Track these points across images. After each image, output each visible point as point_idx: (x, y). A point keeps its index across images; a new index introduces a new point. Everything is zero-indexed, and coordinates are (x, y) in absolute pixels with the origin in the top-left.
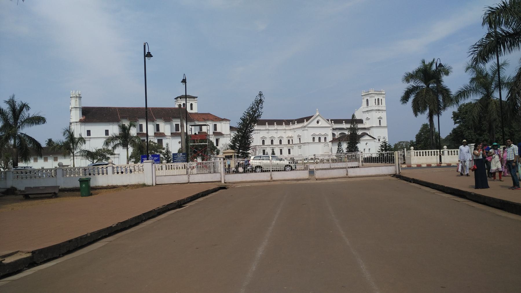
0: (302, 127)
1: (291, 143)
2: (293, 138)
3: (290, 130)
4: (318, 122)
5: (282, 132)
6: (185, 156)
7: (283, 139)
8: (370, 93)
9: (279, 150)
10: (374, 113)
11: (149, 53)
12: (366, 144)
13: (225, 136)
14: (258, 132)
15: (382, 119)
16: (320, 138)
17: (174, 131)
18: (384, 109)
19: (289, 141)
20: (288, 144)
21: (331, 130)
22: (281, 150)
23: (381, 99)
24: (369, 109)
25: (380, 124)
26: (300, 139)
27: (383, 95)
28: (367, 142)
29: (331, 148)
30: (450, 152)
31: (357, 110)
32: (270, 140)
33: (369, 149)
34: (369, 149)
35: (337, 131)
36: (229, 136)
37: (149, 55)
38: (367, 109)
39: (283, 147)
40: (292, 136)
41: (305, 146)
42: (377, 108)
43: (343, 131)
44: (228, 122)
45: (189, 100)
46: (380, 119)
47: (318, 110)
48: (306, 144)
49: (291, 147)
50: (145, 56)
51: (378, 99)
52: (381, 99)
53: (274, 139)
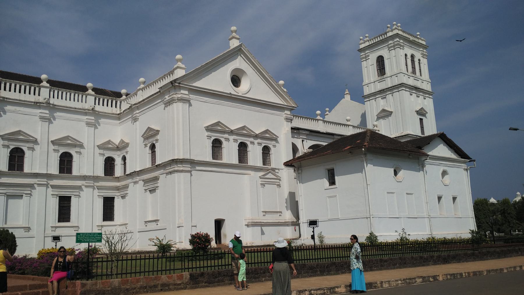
0: (161, 93)
2: (128, 149)
3: (119, 117)
4: (236, 80)
5: (80, 120)
7: (80, 153)
8: (390, 34)
10: (405, 94)
16: (243, 148)
18: (427, 87)
20: (106, 174)
23: (419, 60)
24: (389, 83)
25: (423, 132)
26: (153, 147)
27: (421, 49)
28: (446, 168)
29: (292, 195)
31: (330, 111)
32: (4, 146)
34: (454, 199)
38: (380, 86)
39: (79, 188)
40: (122, 141)
41: (176, 175)
42: (411, 82)
46: (421, 113)
47: (235, 32)
48: (180, 167)
49: (118, 189)
51: (412, 56)
52: (419, 60)
53: (33, 149)
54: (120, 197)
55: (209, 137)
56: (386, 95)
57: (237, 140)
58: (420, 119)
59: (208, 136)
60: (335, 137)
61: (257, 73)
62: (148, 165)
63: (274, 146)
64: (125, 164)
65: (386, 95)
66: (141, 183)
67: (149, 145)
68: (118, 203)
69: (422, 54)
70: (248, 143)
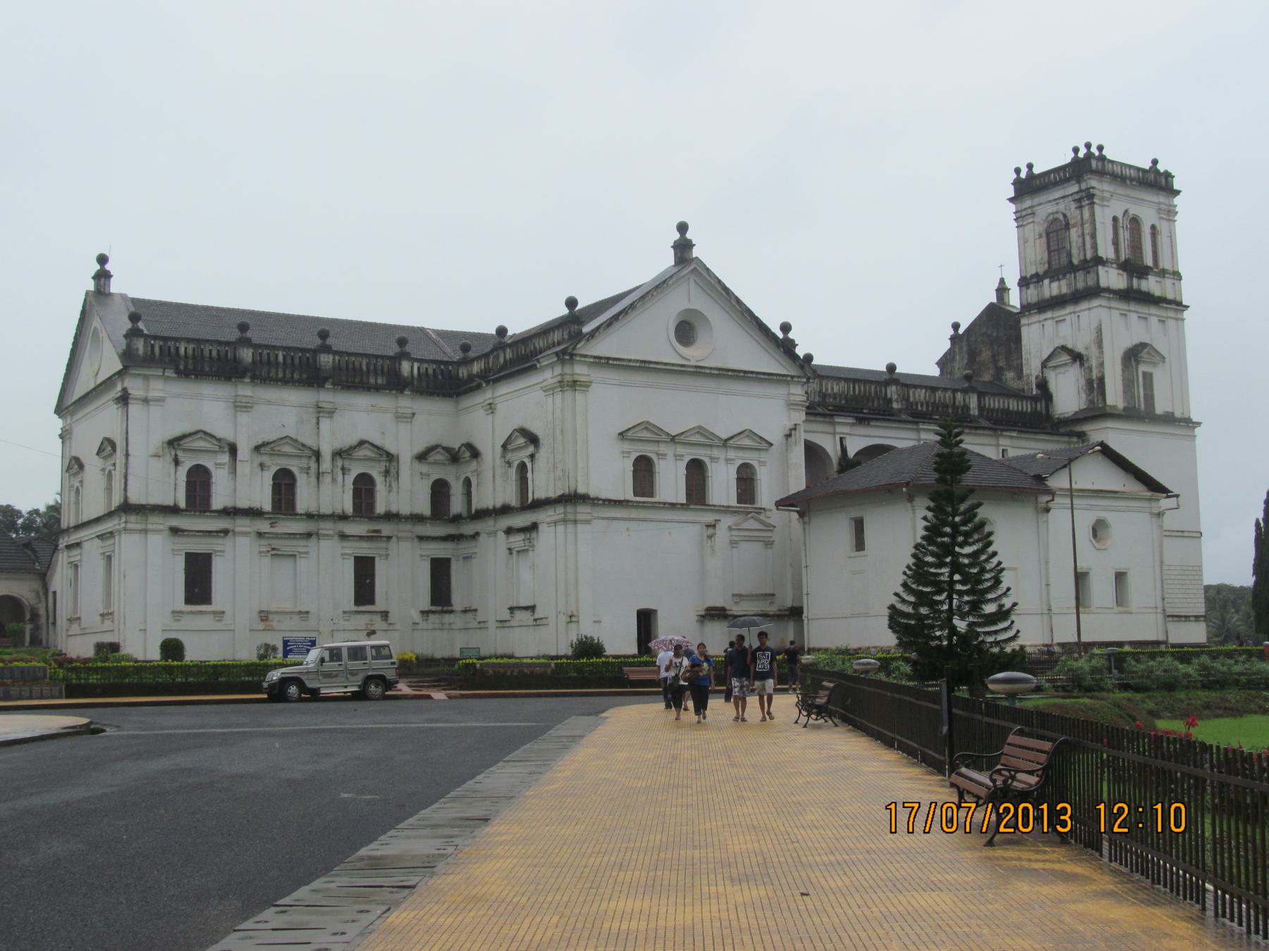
1: (457, 505)
4: (685, 331)
9: (348, 569)
12: (1095, 536)
14: (157, 388)
16: (696, 471)
19: (440, 491)
21: (791, 405)
22: (364, 571)
23: (1153, 227)
26: (522, 468)
33: (1120, 577)
34: (1120, 577)
35: (844, 426)
51: (1135, 221)
52: (1153, 227)
54: (461, 559)
55: (625, 454)
56: (1066, 315)
57: (683, 456)
58: (1144, 374)
59: (623, 452)
60: (921, 427)
61: (731, 313)
62: (514, 502)
64: (468, 494)
65: (1066, 315)
66: (501, 535)
67: (516, 464)
68: (457, 572)
69: (1159, 211)
70: (706, 460)
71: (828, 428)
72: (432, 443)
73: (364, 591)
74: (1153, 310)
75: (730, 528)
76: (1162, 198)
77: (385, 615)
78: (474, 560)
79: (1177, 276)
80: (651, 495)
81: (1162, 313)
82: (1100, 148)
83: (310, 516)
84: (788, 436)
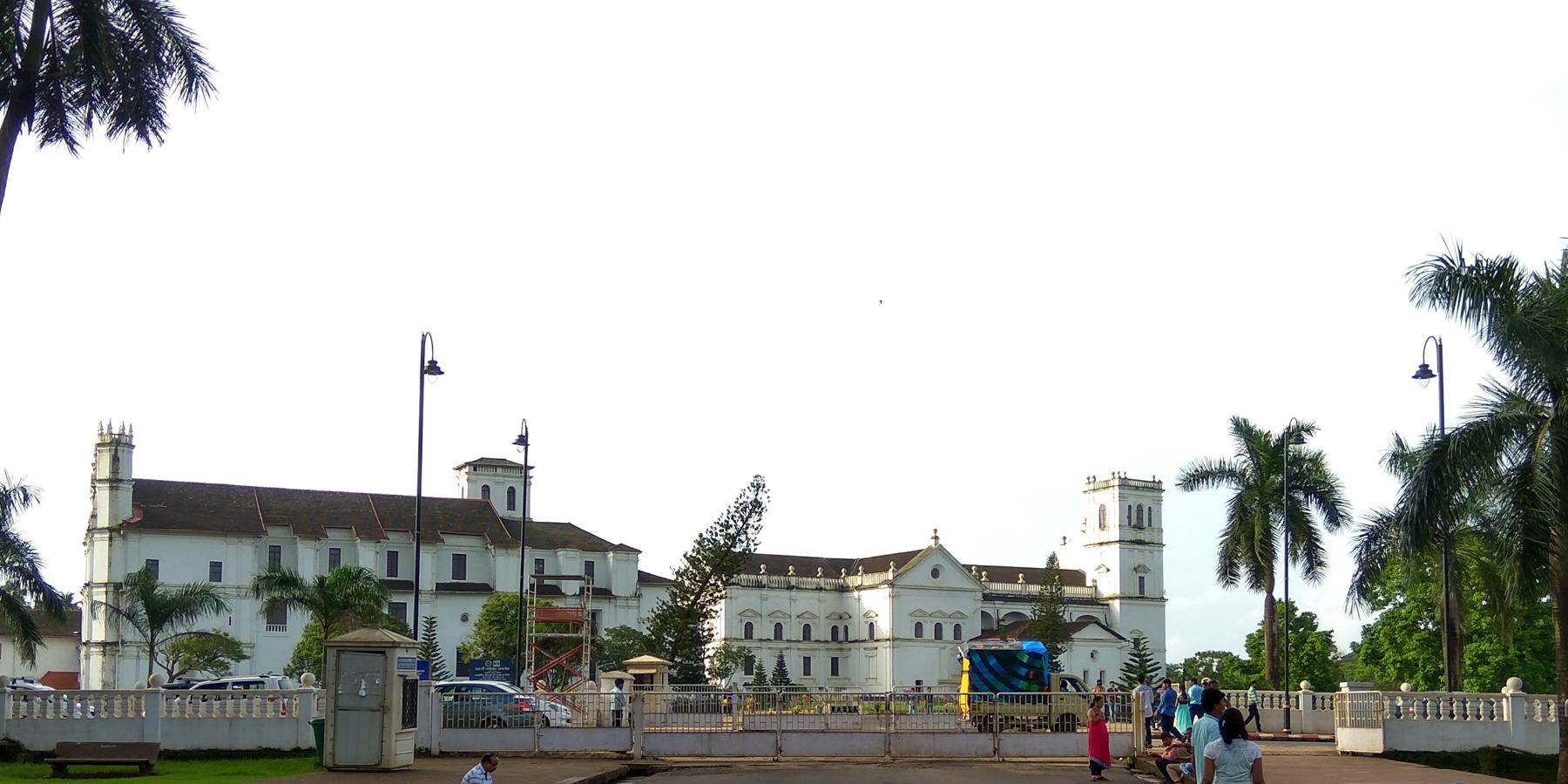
1: (841, 636)
6: (508, 669)
11: (433, 363)
12: (1092, 656)
13: (619, 603)
15: (1146, 569)
16: (938, 628)
17: (448, 579)
19: (835, 629)
21: (975, 600)
22: (807, 661)
23: (1150, 508)
28: (1095, 649)
30: (1319, 701)
35: (998, 604)
36: (634, 603)
37: (432, 368)
43: (1016, 606)
44: (632, 556)
45: (505, 476)
50: (423, 372)
51: (1140, 508)
52: (1150, 508)
63: (964, 624)
71: (993, 606)
72: (831, 612)
73: (807, 672)
74: (1146, 547)
75: (951, 649)
76: (1155, 494)
77: (814, 679)
78: (849, 659)
79: (1161, 530)
80: (922, 637)
81: (1151, 548)
82: (1125, 473)
83: (788, 641)
84: (975, 612)
